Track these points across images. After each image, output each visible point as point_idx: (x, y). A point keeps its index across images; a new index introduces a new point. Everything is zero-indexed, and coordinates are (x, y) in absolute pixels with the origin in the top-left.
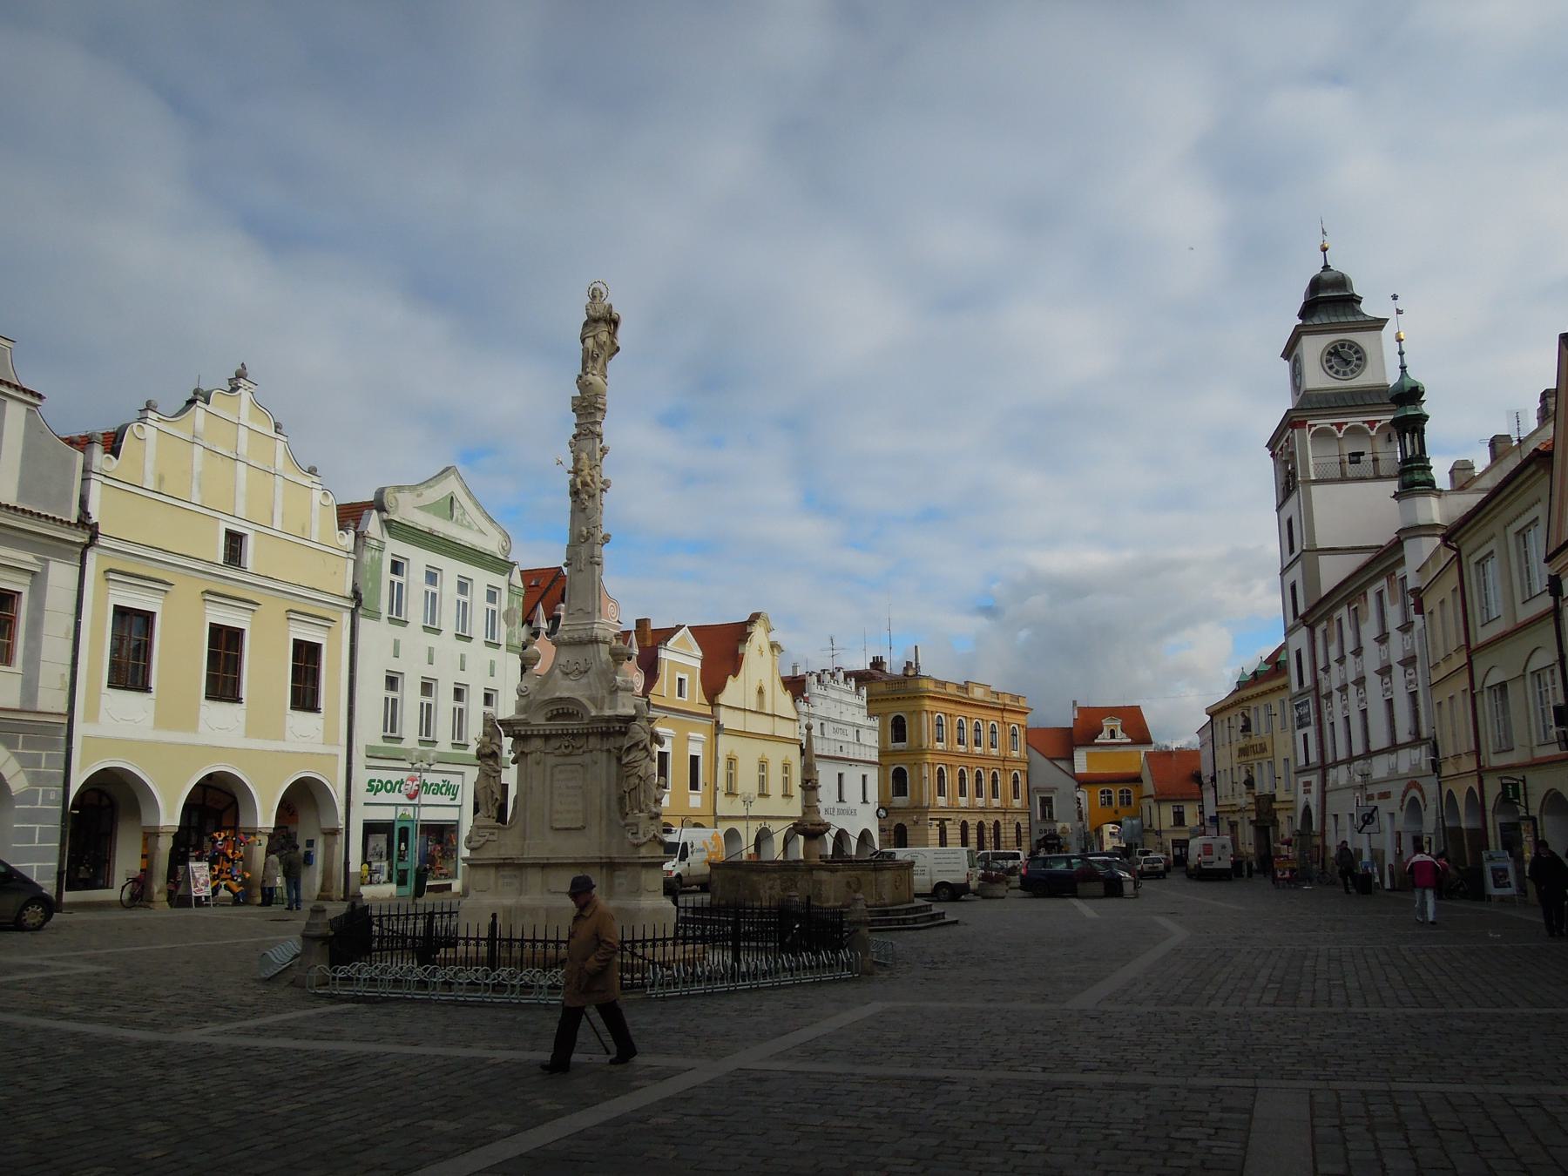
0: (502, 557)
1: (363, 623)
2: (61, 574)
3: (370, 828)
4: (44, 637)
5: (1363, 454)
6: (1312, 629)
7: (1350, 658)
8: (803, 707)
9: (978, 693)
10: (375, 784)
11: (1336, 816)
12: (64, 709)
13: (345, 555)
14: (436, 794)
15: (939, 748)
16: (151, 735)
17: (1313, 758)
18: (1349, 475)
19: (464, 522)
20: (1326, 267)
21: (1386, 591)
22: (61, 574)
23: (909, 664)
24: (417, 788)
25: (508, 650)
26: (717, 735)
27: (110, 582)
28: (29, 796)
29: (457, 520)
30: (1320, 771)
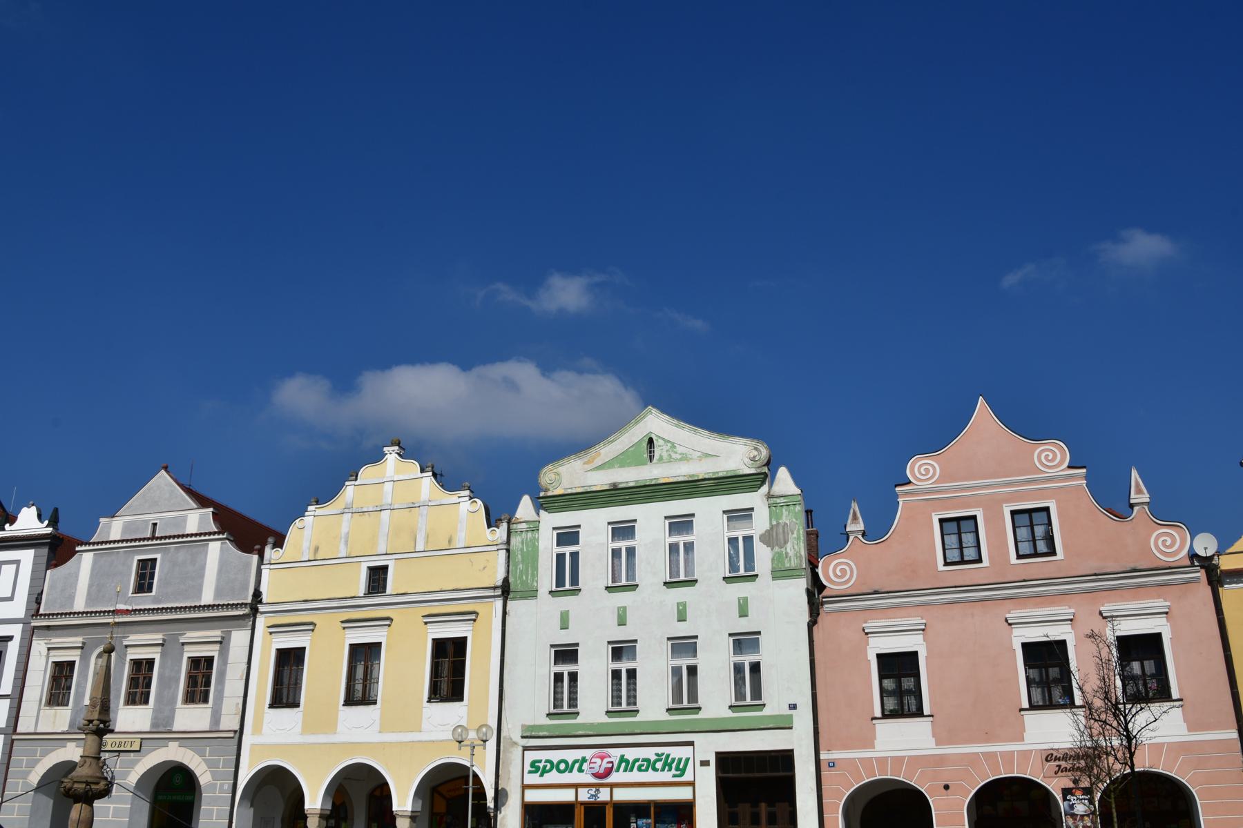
0: (753, 471)
2: (239, 638)
4: (227, 681)
10: (541, 765)
12: (237, 727)
13: (495, 548)
14: (647, 770)
16: (299, 739)
19: (674, 456)
22: (239, 638)
24: (610, 765)
25: (774, 578)
27: (273, 635)
28: (212, 787)
29: (661, 458)
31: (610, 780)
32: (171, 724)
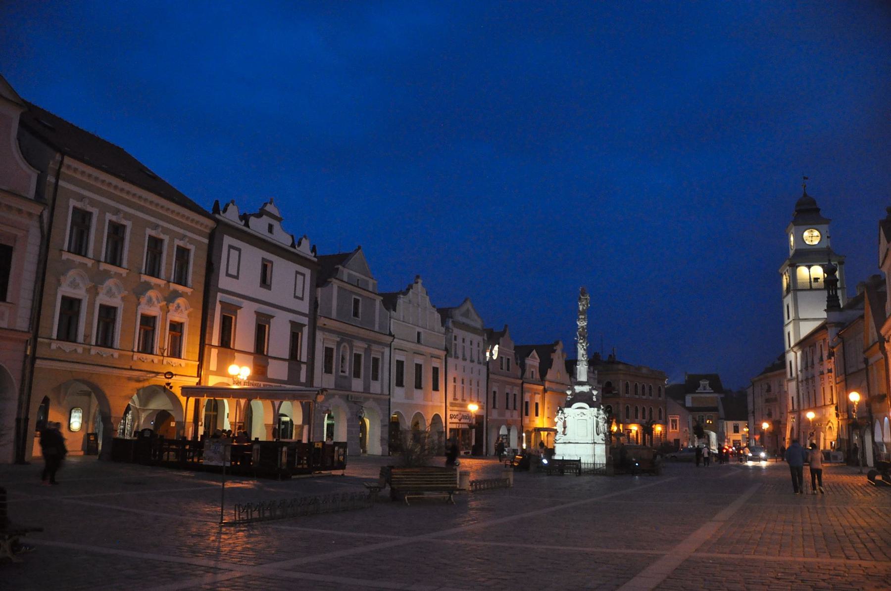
1: (449, 359)
2: (387, 350)
3: (451, 430)
5: (819, 278)
6: (796, 353)
7: (809, 369)
8: (572, 379)
9: (644, 371)
11: (804, 432)
15: (627, 396)
17: (795, 407)
18: (800, 318)
20: (805, 195)
21: (823, 346)
23: (610, 356)
25: (484, 365)
26: (544, 393)
30: (798, 413)
31: (461, 422)
32: (369, 390)
